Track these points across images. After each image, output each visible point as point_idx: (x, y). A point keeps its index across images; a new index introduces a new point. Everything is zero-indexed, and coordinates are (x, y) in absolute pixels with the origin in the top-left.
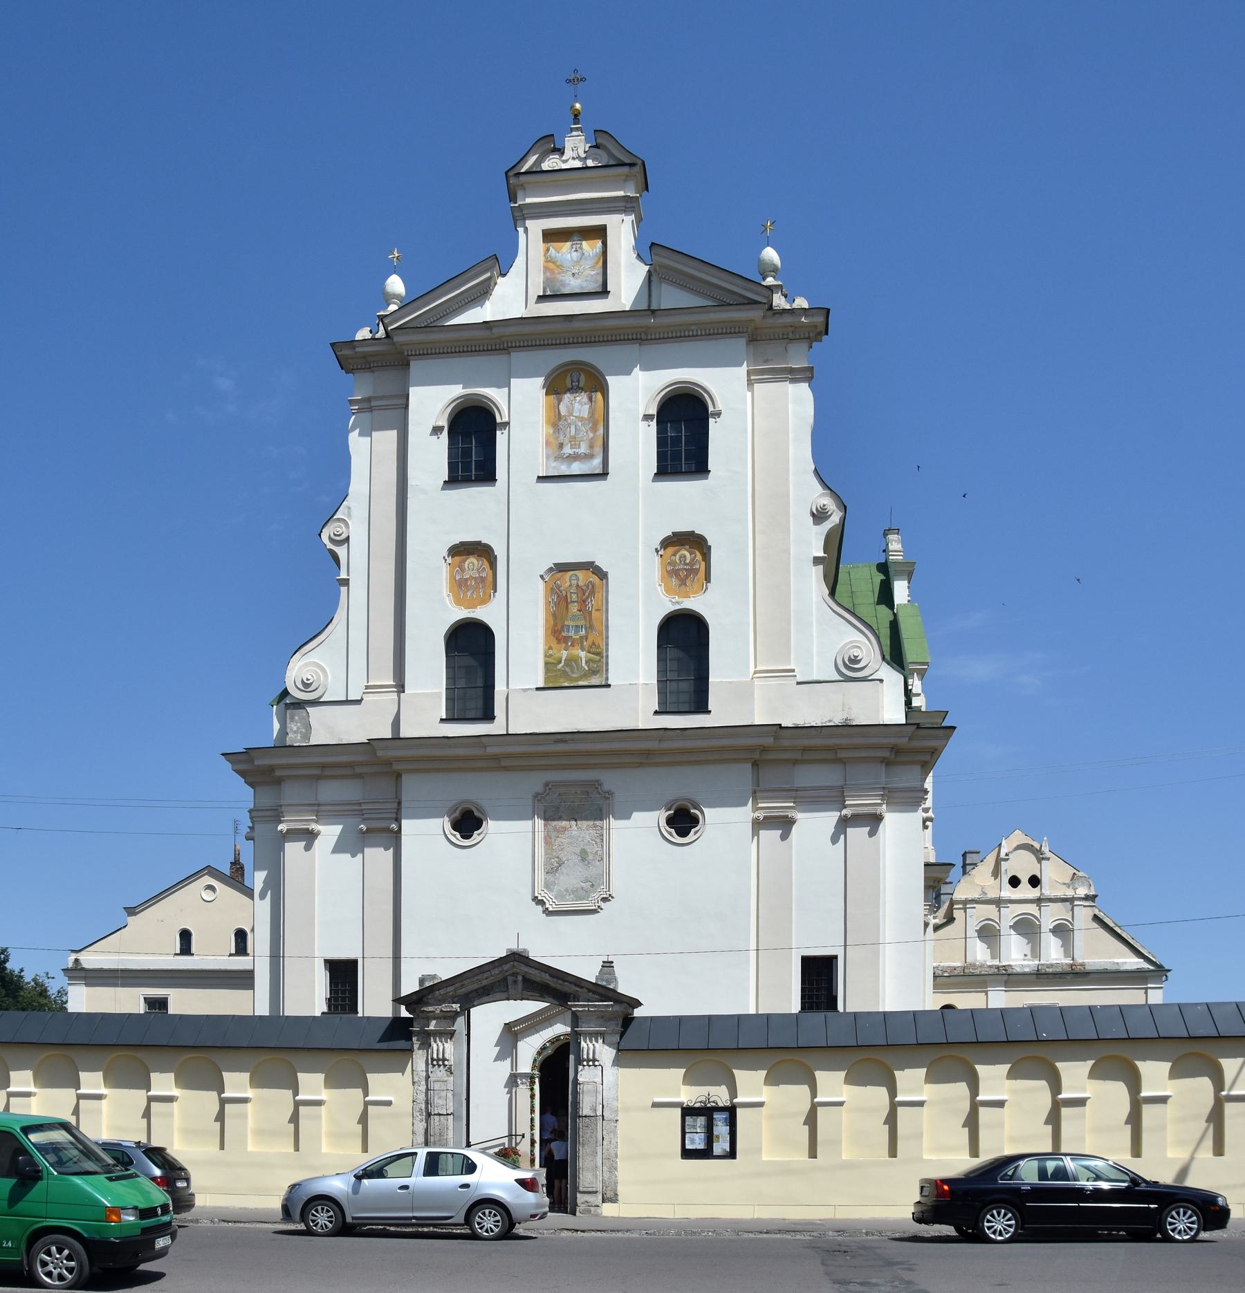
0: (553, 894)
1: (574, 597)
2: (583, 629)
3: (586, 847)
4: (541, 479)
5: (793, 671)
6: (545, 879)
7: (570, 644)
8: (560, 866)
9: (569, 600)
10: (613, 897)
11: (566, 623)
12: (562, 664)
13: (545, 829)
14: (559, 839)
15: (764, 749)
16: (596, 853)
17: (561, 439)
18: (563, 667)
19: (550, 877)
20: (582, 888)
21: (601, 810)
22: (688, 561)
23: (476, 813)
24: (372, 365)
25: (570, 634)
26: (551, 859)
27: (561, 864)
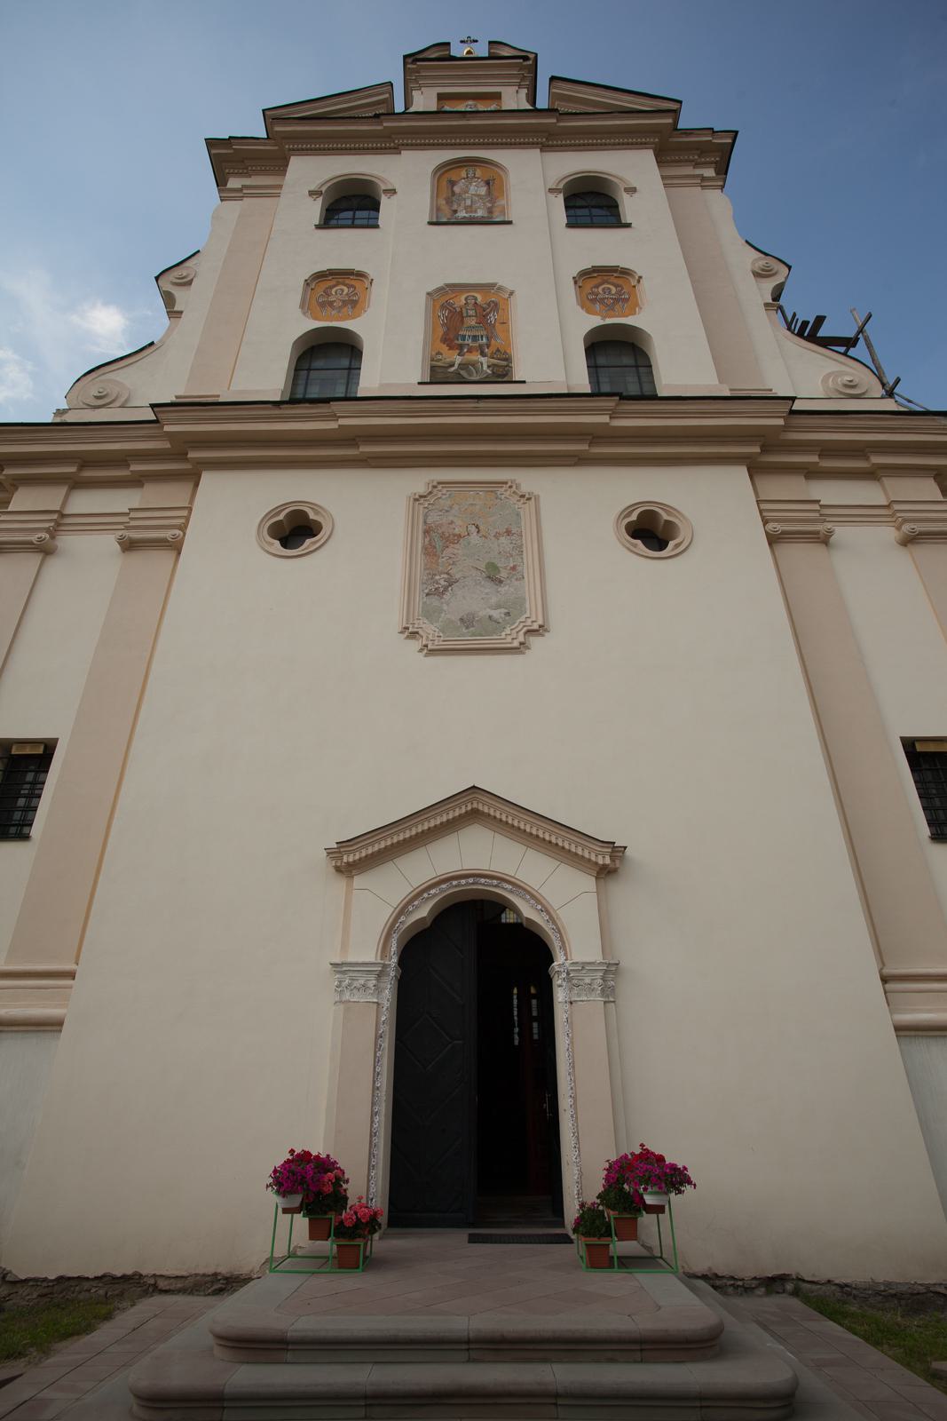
0: (437, 624)
1: (472, 313)
2: (484, 339)
3: (495, 561)
4: (431, 223)
5: (771, 390)
6: (424, 603)
7: (465, 350)
8: (450, 586)
9: (465, 315)
10: (546, 631)
11: (461, 333)
12: (452, 369)
13: (425, 537)
14: (448, 552)
15: (769, 441)
16: (514, 568)
17: (455, 207)
18: (457, 370)
19: (434, 601)
20: (490, 617)
21: (518, 515)
22: (613, 292)
23: (312, 516)
24: (250, 168)
25: (466, 342)
26: (435, 575)
27: (451, 583)
